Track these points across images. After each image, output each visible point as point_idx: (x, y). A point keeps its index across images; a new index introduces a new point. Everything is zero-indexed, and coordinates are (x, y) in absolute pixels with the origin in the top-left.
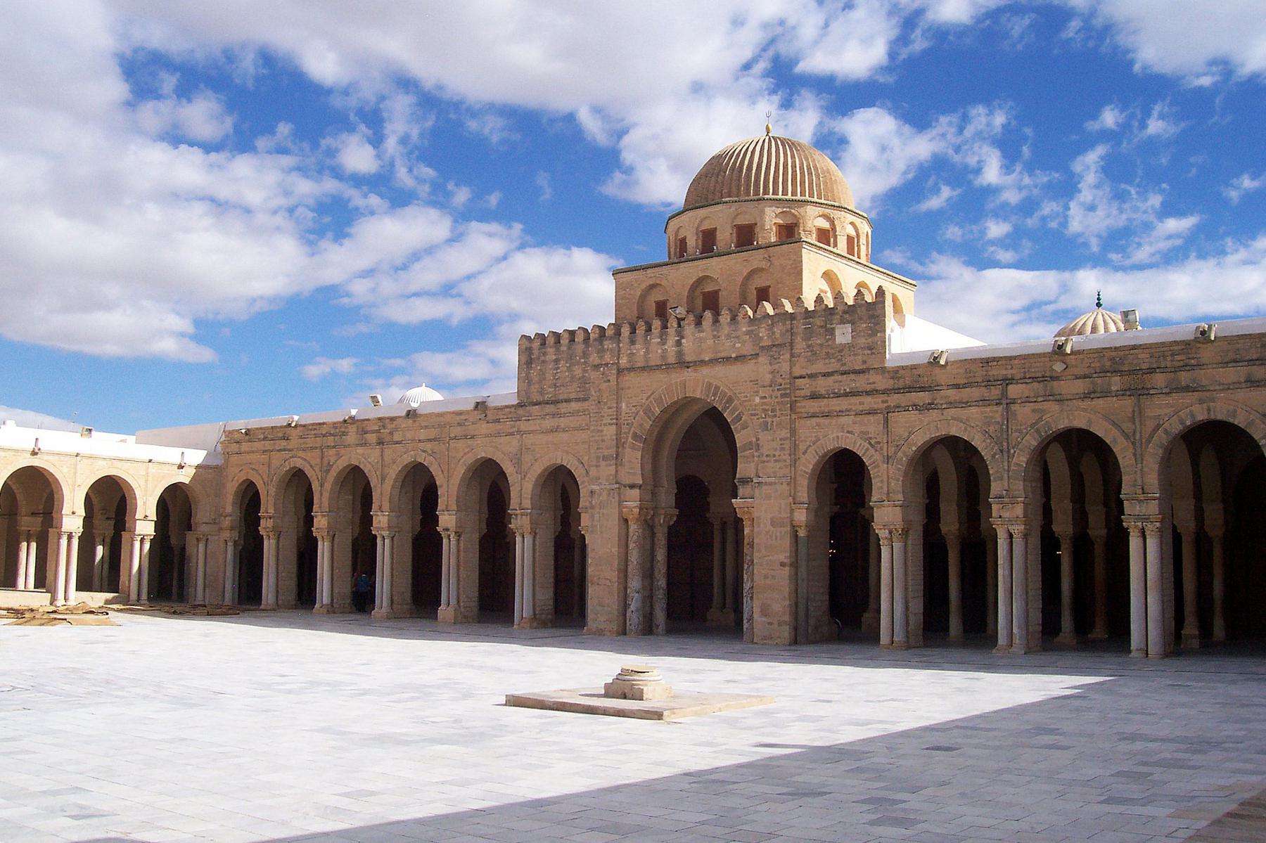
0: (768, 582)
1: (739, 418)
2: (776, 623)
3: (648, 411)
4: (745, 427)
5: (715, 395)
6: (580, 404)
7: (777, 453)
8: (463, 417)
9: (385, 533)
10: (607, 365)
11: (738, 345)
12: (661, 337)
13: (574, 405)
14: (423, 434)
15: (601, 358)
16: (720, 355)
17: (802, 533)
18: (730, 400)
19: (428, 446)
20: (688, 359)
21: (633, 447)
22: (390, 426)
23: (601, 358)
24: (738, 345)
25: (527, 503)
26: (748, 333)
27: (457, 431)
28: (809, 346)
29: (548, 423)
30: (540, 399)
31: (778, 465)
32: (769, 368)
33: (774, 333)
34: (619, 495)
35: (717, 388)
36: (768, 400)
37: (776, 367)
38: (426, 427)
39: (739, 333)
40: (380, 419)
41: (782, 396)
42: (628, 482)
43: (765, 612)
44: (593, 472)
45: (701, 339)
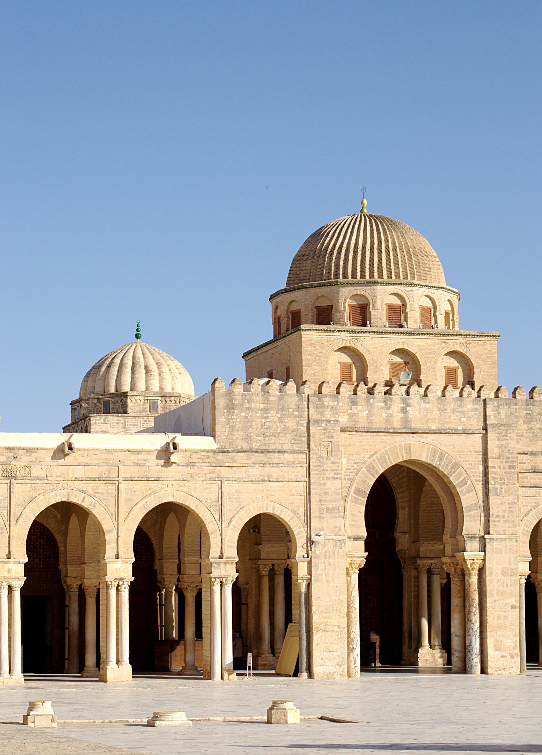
0: (502, 622)
2: (508, 656)
5: (440, 460)
6: (295, 456)
7: (506, 515)
8: (142, 457)
9: (13, 584)
10: (329, 421)
11: (463, 419)
12: (385, 402)
13: (288, 457)
14: (79, 472)
15: (321, 414)
16: (446, 426)
17: (523, 581)
18: (456, 465)
19: (89, 486)
20: (415, 425)
21: (356, 501)
22: (25, 460)
23: (321, 414)
24: (463, 419)
25: (232, 552)
26: (475, 410)
27: (135, 472)
28: (531, 428)
29: (257, 472)
30: (246, 446)
31: (507, 525)
32: (497, 443)
33: (499, 414)
35: (442, 455)
36: (497, 470)
37: (504, 442)
38: (87, 465)
39: (464, 409)
40: (9, 449)
41: (509, 467)
43: (497, 648)
45: (427, 410)
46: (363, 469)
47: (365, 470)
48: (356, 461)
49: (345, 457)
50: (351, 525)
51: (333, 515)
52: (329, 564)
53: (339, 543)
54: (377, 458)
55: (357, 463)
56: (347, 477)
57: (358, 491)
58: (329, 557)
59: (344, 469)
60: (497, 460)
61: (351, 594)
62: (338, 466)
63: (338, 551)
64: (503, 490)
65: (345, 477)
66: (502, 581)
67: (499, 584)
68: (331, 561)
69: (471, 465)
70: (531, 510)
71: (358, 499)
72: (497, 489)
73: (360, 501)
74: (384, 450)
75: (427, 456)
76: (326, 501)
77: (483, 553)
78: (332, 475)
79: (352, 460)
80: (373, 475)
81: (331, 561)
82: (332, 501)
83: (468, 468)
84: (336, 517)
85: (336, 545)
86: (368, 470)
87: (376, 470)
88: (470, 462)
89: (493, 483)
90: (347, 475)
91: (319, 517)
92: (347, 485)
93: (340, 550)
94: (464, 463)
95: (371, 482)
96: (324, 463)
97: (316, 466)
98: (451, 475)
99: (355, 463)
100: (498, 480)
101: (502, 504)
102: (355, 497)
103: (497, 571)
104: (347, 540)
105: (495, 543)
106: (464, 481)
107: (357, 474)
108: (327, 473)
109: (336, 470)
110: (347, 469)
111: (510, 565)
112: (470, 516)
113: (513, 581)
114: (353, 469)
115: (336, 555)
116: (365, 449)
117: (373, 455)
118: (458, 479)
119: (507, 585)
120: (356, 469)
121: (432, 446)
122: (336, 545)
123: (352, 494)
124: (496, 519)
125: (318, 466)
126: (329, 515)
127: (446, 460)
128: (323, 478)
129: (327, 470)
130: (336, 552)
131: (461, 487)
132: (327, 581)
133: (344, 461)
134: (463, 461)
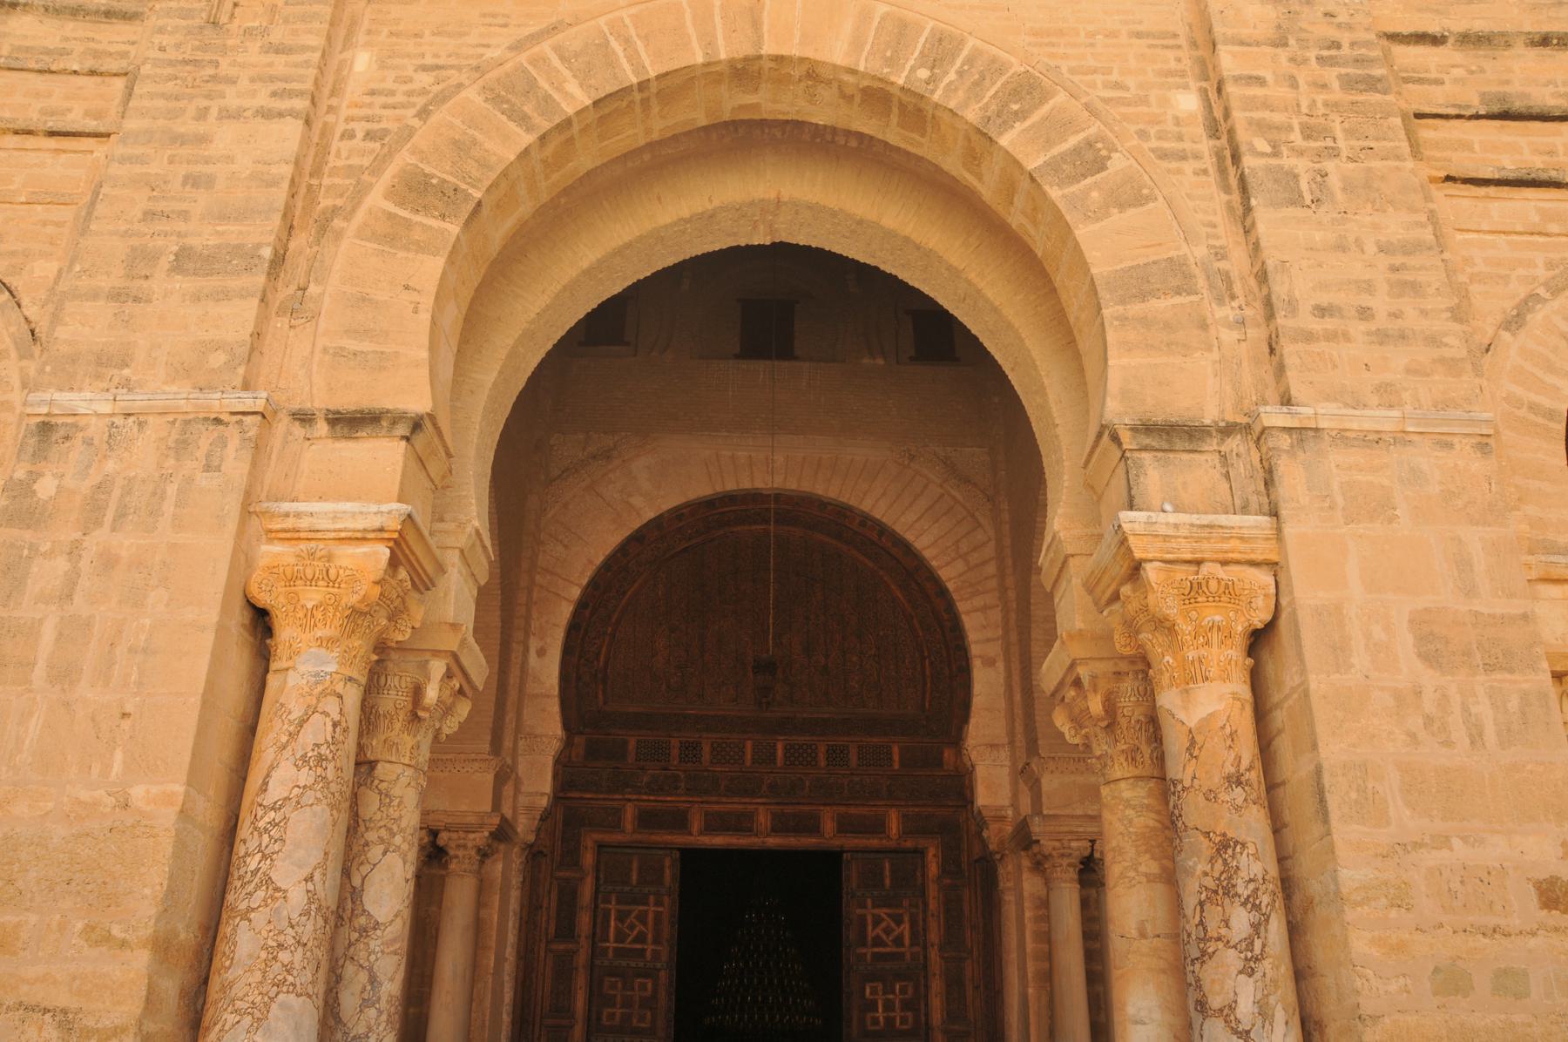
1: (1090, 160)
3: (511, 94)
4: (1132, 196)
7: (1381, 303)
21: (392, 235)
34: (258, 448)
42: (320, 401)
44: (86, 326)
46: (472, 94)
47: (479, 100)
48: (429, 60)
49: (367, 45)
50: (340, 353)
51: (213, 283)
52: (108, 562)
53: (205, 439)
54: (557, 49)
55: (438, 67)
56: (360, 128)
57: (417, 190)
58: (121, 515)
59: (353, 90)
60: (1268, 50)
61: (264, 788)
62: (307, 63)
63: (190, 480)
64: (1334, 181)
65: (352, 125)
66: (1429, 705)
67: (1415, 723)
68: (126, 543)
69: (1117, 86)
70: (1534, 297)
71: (408, 224)
72: (1296, 176)
73: (417, 235)
74: (602, 21)
75: (857, 44)
76: (185, 215)
77: (1264, 520)
78: (263, 99)
79: (408, 56)
80: (523, 120)
81: (126, 543)
82: (223, 217)
83: (1106, 101)
84: (224, 295)
85: (182, 447)
86: (496, 100)
87: (548, 98)
88: (1115, 77)
89: (1262, 145)
90: (368, 119)
91: (116, 296)
92: (355, 161)
93: (203, 480)
94: (1076, 78)
95: (507, 143)
96: (224, 50)
97: (171, 63)
98: (1006, 126)
99: (425, 68)
100: (1296, 137)
101: (1341, 247)
102: (391, 216)
103: (1378, 632)
104: (283, 424)
105: (1336, 458)
106: (1089, 156)
107: (424, 113)
108: (230, 91)
109: (286, 80)
110: (372, 93)
111: (1470, 591)
112: (1145, 322)
113: (1514, 704)
114: (409, 94)
115: (169, 507)
116: (494, 16)
117: (535, 38)
118: (1049, 143)
119: (1476, 737)
120: (424, 92)
121: (882, 9)
122: (182, 447)
123: (376, 199)
124: (1317, 325)
125: (186, 62)
126: (182, 283)
127: (970, 61)
128: (202, 114)
129: (232, 81)
130: (172, 490)
131: (1075, 179)
132: (64, 674)
133: (362, 61)
134: (1072, 71)
